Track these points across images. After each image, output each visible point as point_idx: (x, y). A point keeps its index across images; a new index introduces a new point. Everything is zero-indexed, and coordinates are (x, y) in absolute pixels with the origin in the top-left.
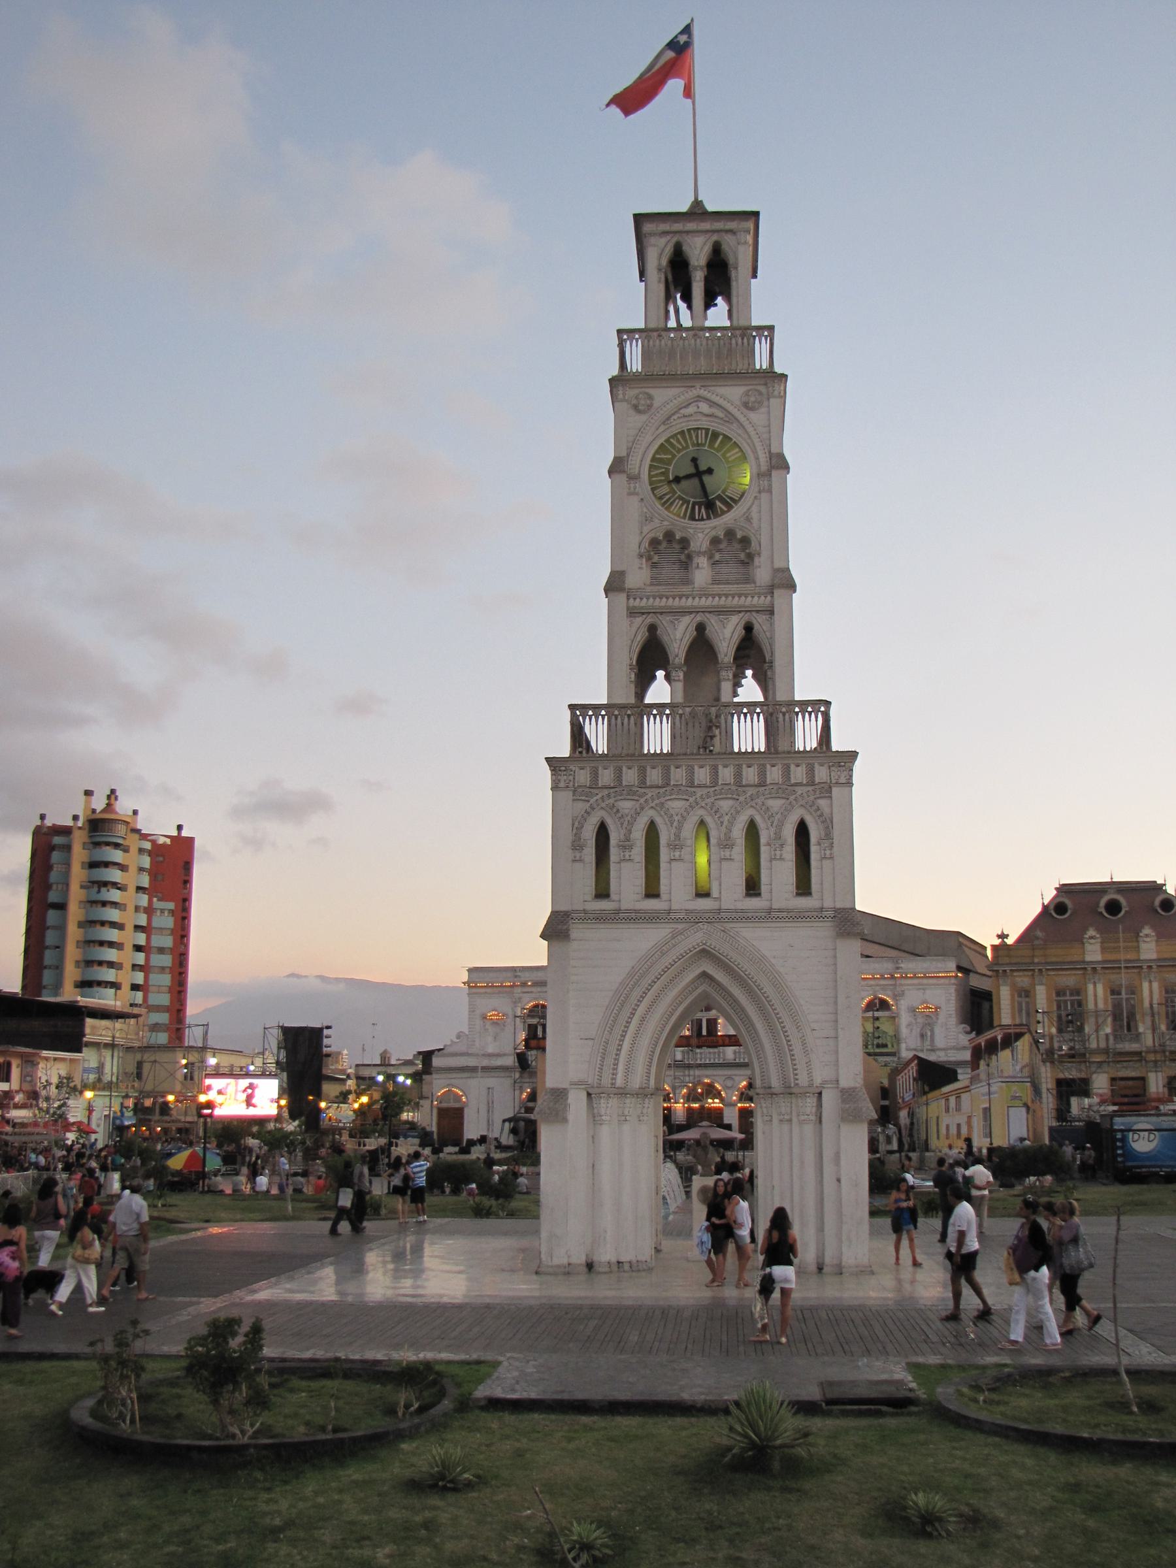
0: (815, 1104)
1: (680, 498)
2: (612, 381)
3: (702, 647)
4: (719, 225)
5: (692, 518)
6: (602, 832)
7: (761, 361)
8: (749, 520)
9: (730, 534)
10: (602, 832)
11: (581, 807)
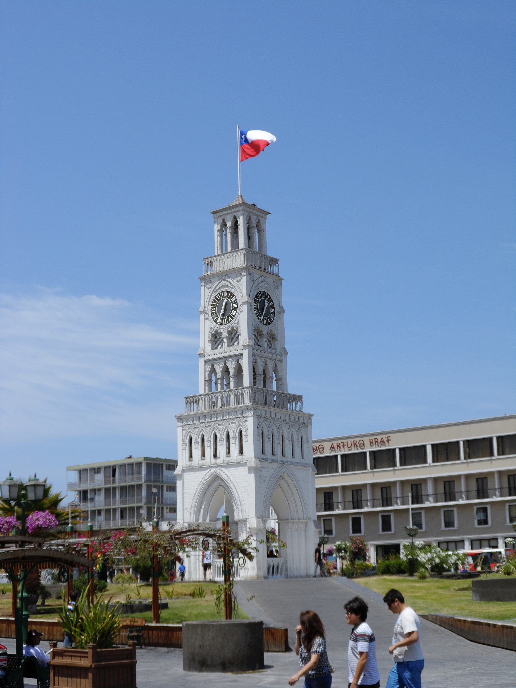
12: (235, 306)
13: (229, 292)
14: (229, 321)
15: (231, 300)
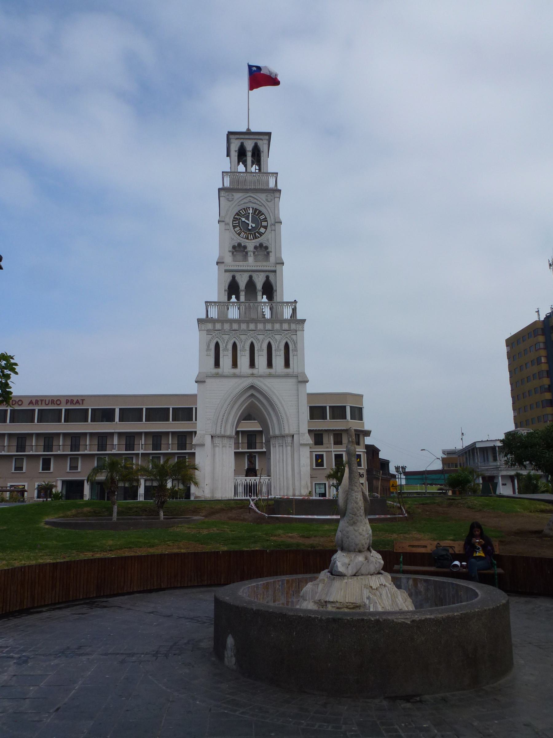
0: (291, 440)
1: (243, 231)
2: (220, 190)
3: (251, 285)
4: (257, 137)
5: (248, 239)
6: (217, 346)
7: (272, 185)
8: (268, 240)
9: (261, 245)
10: (217, 346)
11: (210, 336)
12: (264, 224)
13: (256, 210)
14: (255, 237)
15: (259, 217)
